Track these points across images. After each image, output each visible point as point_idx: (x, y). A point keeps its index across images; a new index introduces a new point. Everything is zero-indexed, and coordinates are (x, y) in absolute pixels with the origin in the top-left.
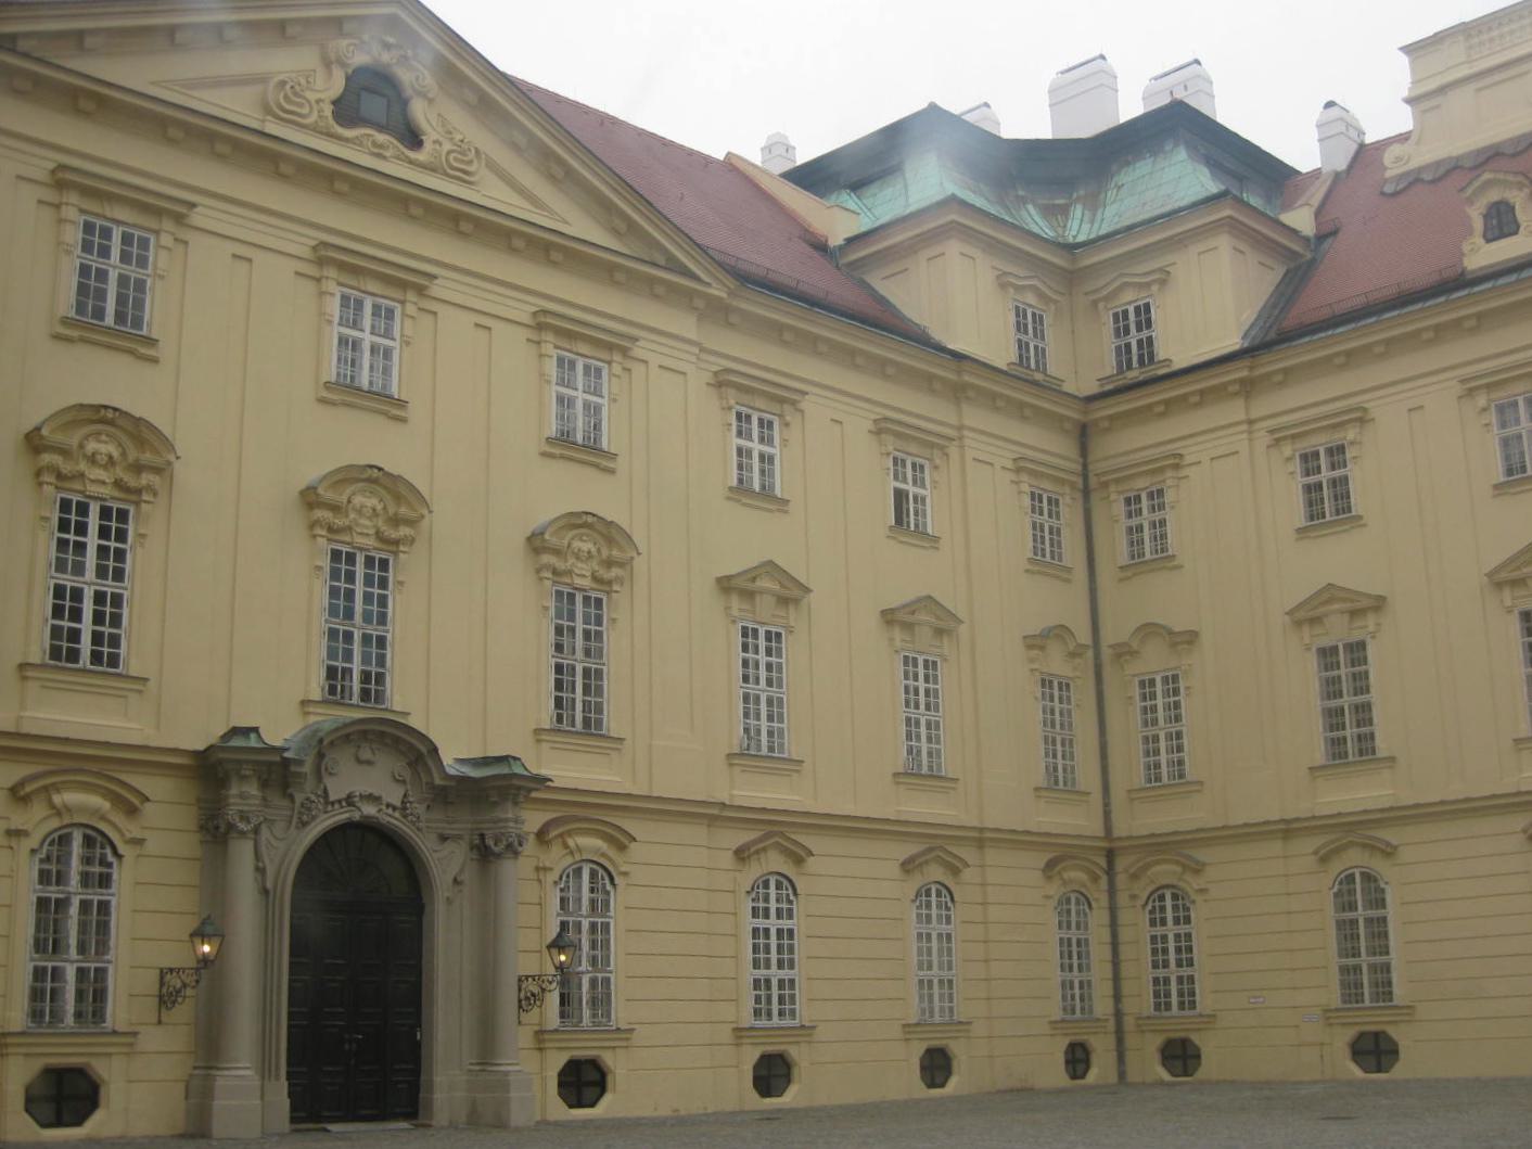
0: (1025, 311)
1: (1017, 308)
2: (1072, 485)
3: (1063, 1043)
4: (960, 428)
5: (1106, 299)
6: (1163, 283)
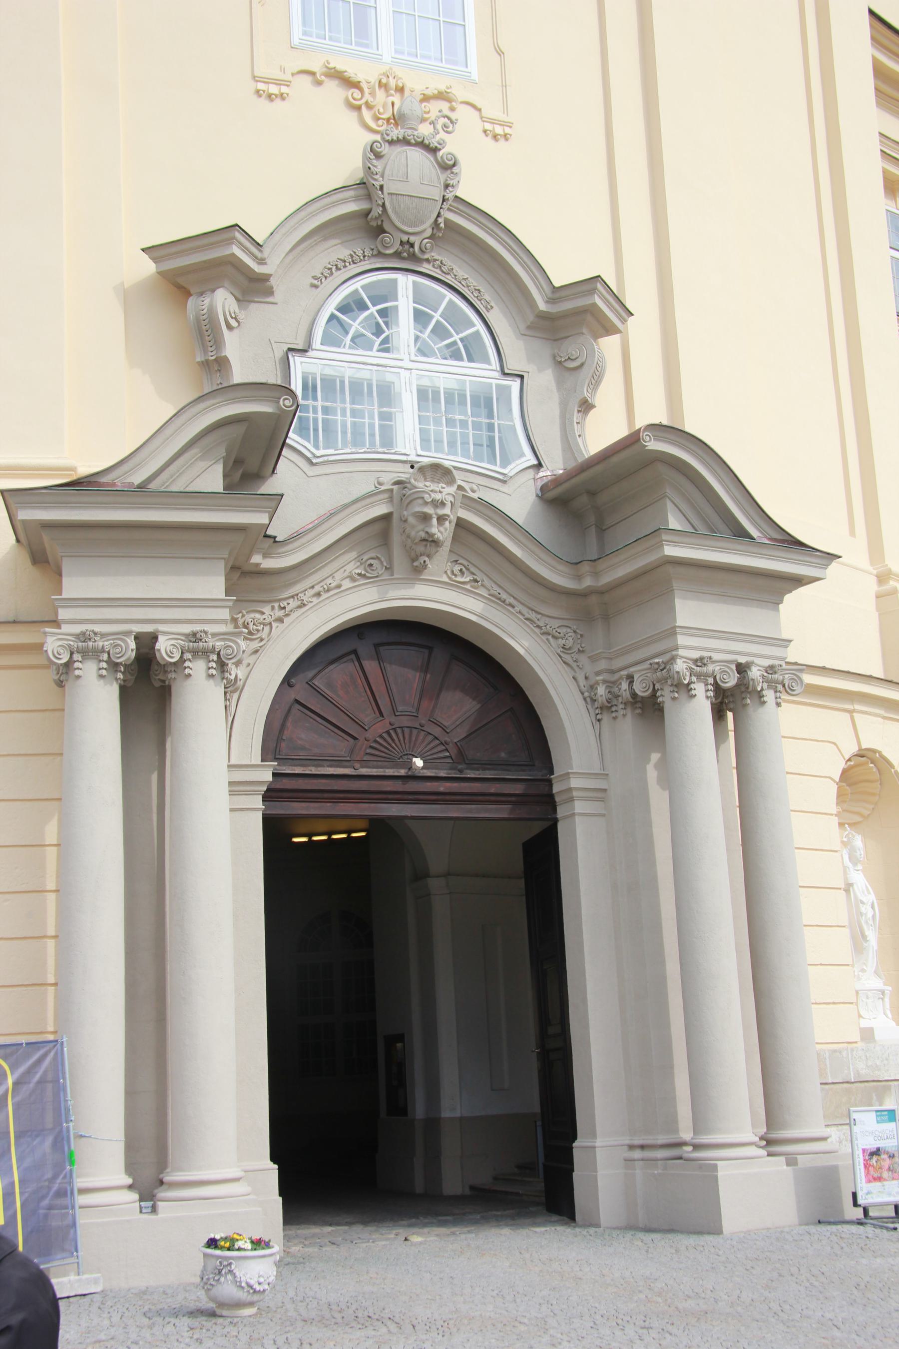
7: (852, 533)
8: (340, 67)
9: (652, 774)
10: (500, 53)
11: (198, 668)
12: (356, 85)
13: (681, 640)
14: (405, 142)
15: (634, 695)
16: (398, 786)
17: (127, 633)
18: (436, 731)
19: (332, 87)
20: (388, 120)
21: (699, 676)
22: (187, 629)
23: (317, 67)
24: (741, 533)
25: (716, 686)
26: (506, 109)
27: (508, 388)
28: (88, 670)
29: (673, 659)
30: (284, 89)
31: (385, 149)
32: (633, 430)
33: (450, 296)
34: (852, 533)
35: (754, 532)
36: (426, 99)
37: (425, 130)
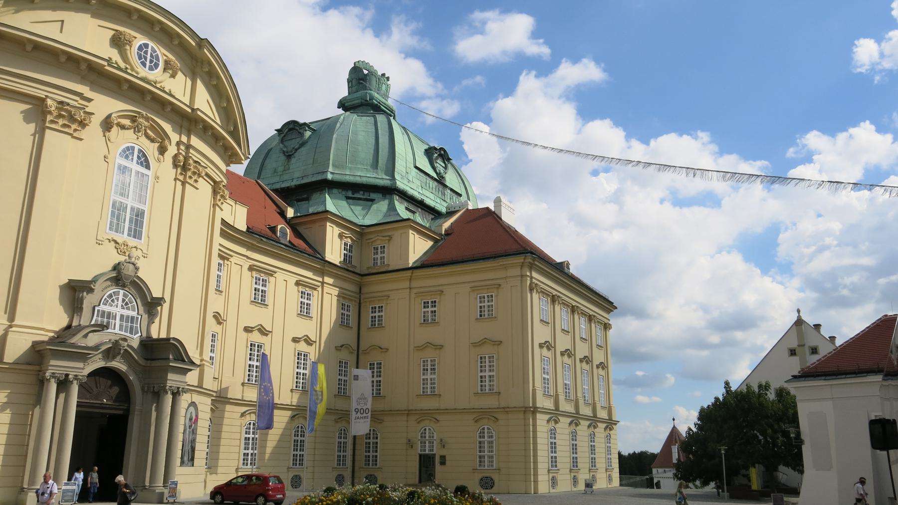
0: (347, 244)
1: (345, 243)
2: (355, 301)
3: (335, 474)
4: (323, 283)
5: (372, 242)
6: (389, 240)
7: (197, 349)
8: (116, 239)
9: (154, 408)
10: (148, 237)
11: (75, 382)
12: (118, 244)
13: (168, 382)
14: (129, 263)
15: (153, 390)
16: (99, 405)
17: (63, 374)
18: (108, 393)
19: (113, 243)
20: (123, 252)
21: (170, 390)
22: (75, 374)
23: (110, 238)
24: (183, 361)
25: (172, 392)
26: (147, 251)
27: (138, 318)
28: (53, 380)
29: (166, 386)
30: (103, 243)
31: (125, 264)
32: (168, 337)
33: (130, 296)
34: (197, 349)
35: (186, 361)
36: (132, 248)
37: (133, 260)
